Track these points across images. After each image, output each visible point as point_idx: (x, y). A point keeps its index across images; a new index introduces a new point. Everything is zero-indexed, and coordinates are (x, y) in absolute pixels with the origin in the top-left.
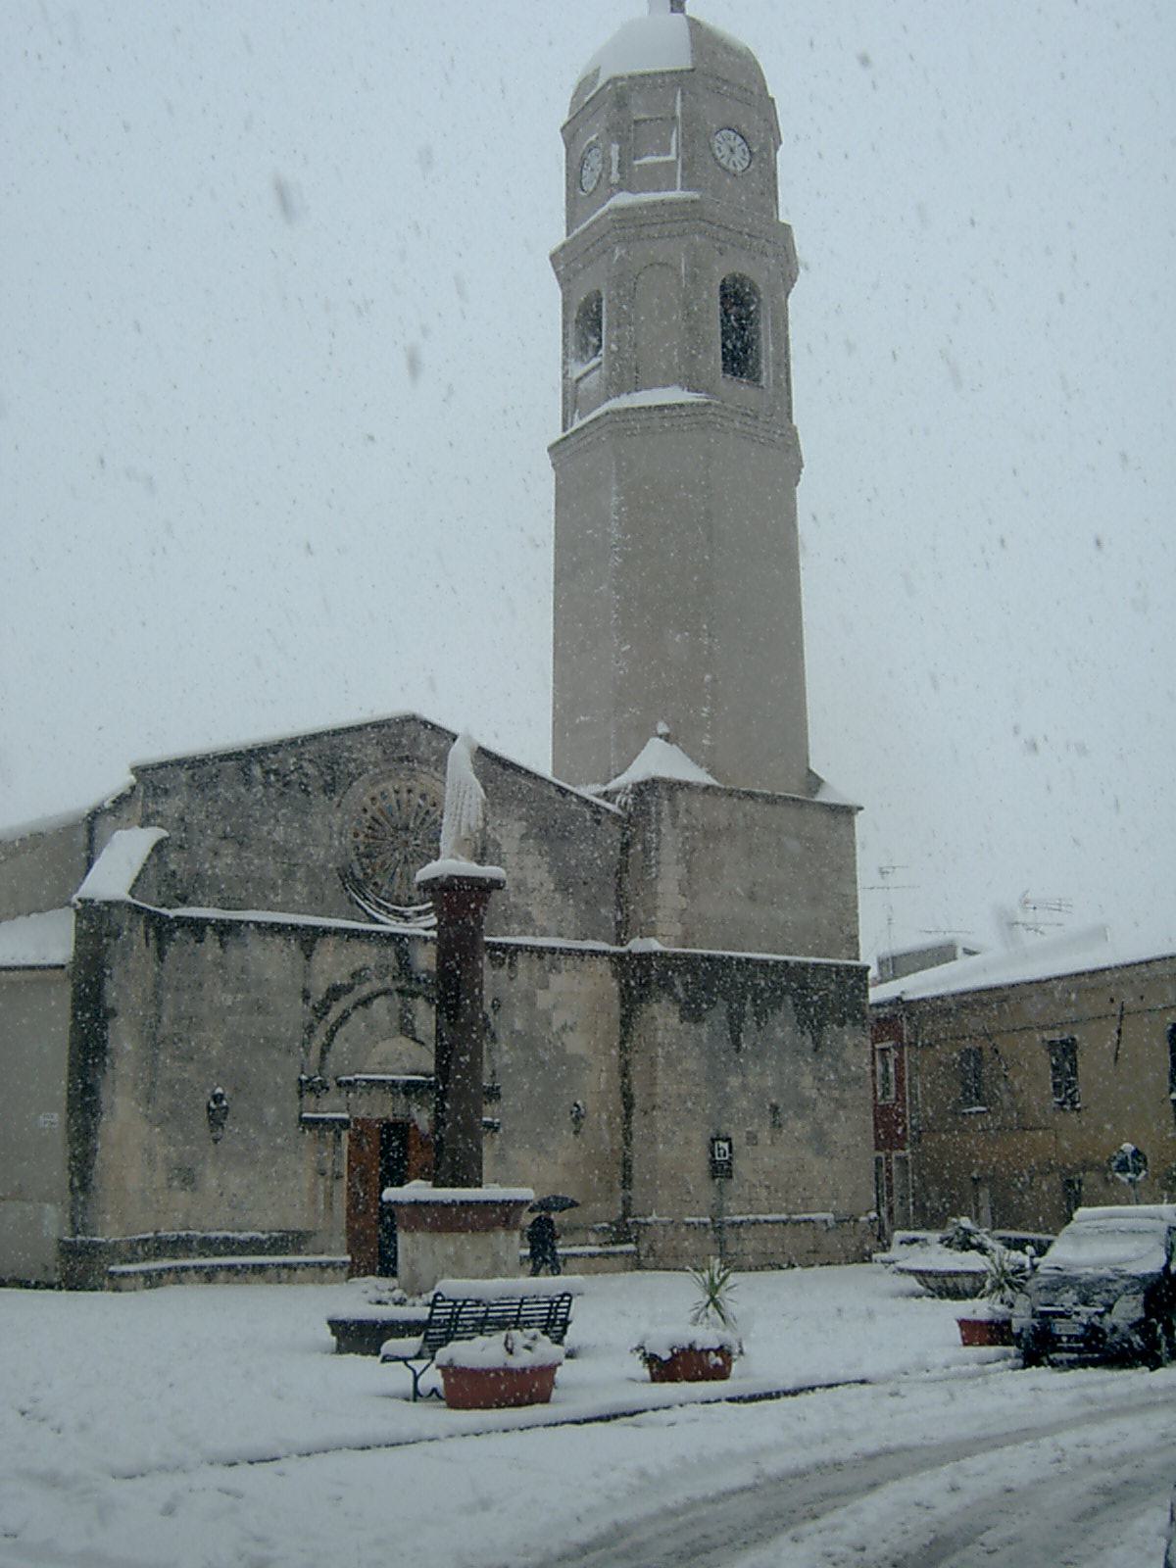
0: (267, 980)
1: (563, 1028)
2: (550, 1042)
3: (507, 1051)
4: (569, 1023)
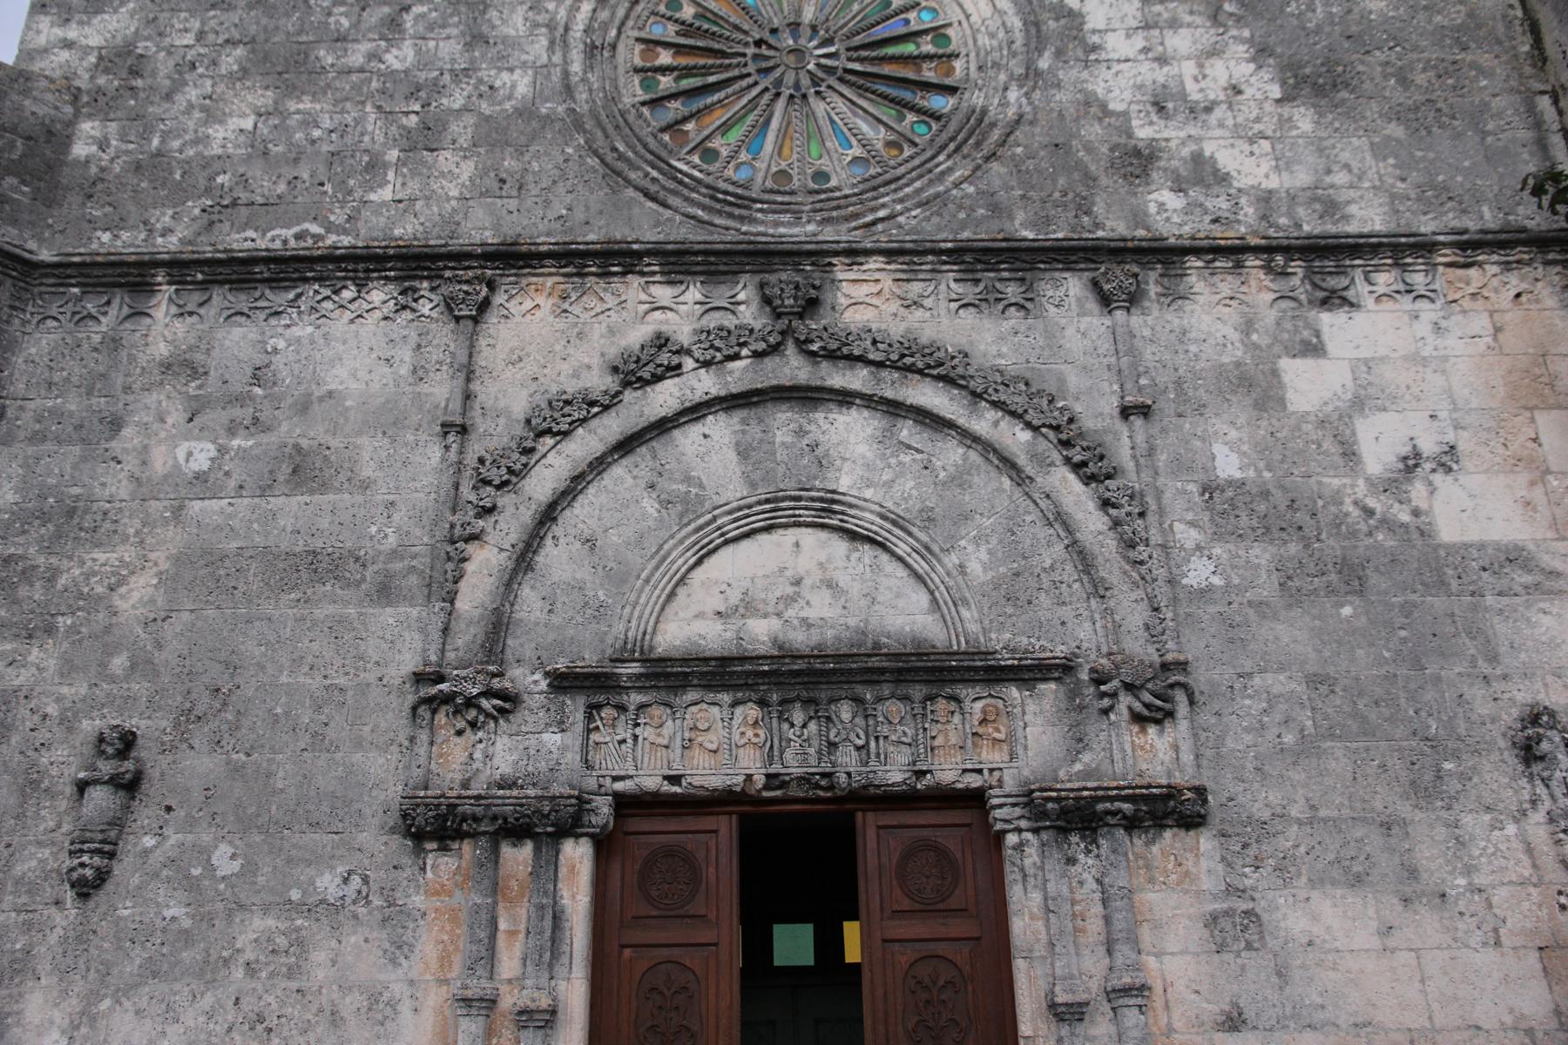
0: (330, 394)
1: (1411, 463)
2: (1369, 512)
3: (1198, 548)
4: (1428, 446)
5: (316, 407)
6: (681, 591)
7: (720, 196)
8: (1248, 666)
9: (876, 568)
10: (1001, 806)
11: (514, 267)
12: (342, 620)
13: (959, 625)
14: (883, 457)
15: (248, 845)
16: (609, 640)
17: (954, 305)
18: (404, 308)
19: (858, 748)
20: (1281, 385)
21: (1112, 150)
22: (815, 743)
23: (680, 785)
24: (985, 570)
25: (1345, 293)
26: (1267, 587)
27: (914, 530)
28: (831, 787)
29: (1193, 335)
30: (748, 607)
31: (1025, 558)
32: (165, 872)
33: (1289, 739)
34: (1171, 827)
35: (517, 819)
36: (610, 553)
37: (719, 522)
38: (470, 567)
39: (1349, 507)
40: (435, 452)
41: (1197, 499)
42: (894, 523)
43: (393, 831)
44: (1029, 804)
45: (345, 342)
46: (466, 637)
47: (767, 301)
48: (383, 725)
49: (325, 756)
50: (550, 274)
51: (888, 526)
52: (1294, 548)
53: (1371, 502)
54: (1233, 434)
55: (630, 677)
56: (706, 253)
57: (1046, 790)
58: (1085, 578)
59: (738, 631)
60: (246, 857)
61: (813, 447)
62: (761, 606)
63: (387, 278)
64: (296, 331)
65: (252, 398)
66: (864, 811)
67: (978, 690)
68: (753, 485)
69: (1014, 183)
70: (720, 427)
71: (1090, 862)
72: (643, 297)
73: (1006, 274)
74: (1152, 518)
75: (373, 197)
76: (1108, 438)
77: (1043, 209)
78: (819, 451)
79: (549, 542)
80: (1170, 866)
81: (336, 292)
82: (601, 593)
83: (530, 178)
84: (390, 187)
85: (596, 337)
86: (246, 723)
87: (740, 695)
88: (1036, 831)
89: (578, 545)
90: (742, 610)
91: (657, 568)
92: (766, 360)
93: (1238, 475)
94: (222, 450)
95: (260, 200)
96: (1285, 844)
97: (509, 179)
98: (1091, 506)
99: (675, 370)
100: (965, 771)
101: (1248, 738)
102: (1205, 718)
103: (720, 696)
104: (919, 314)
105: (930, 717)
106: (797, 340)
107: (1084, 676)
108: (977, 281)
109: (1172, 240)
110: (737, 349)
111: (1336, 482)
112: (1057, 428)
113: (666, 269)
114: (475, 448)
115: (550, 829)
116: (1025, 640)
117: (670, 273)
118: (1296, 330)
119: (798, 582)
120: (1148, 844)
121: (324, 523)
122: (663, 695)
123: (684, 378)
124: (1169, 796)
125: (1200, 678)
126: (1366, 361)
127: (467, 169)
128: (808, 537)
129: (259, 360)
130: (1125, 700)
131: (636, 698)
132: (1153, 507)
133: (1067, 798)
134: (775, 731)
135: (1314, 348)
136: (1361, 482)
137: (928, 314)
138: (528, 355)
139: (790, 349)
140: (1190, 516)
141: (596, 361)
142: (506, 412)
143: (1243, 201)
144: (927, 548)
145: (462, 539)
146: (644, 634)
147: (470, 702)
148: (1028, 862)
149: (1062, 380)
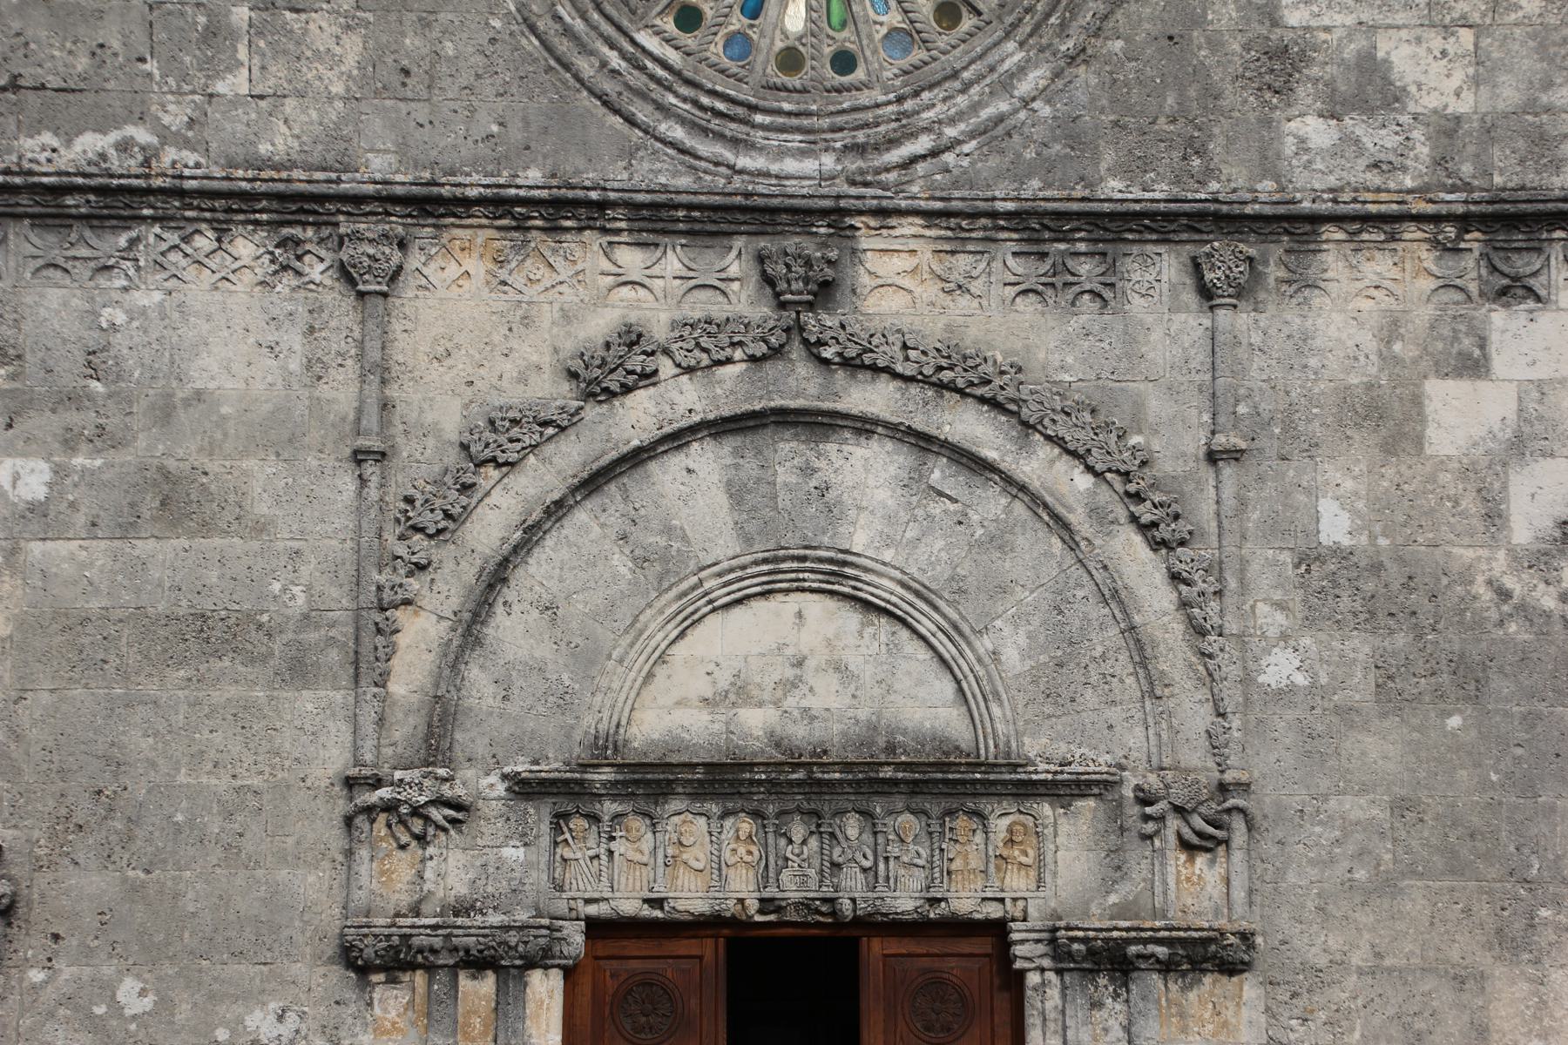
0: (199, 395)
2: (1504, 594)
3: (1284, 637)
5: (181, 413)
6: (661, 671)
7: (705, 100)
8: (1324, 784)
9: (893, 648)
10: (1022, 942)
11: (431, 215)
12: (248, 706)
13: (988, 725)
14: (910, 507)
15: (159, 979)
16: (578, 735)
17: (1011, 291)
18: (285, 268)
19: (864, 870)
20: (1422, 419)
21: (1247, 47)
22: (816, 862)
23: (662, 908)
24: (1023, 660)
25: (1532, 282)
26: (1360, 688)
27: (941, 604)
28: (833, 914)
29: (1318, 343)
30: (740, 692)
31: (1071, 643)
32: (62, 1012)
33: (1361, 874)
34: (1212, 971)
35: (481, 951)
36: (574, 625)
37: (707, 585)
38: (402, 640)
39: (1480, 588)
40: (348, 484)
41: (1290, 572)
42: (918, 594)
43: (331, 961)
44: (1053, 941)
45: (209, 318)
46: (405, 730)
47: (768, 280)
48: (311, 836)
49: (242, 873)
50: (481, 227)
51: (910, 597)
52: (1401, 640)
53: (1509, 582)
54: (1349, 484)
55: (604, 784)
56: (690, 207)
57: (1072, 929)
58: (1140, 671)
59: (727, 723)
60: (158, 993)
61: (823, 490)
62: (755, 692)
63: (257, 223)
64: (141, 298)
65: (91, 397)
66: (869, 937)
67: (1008, 805)
68: (748, 540)
69: (1104, 102)
70: (706, 458)
71: (1118, 1007)
72: (606, 265)
73: (1082, 247)
74: (1230, 600)
75: (220, 87)
76: (1189, 487)
77: (1140, 144)
78: (831, 496)
79: (499, 609)
80: (1207, 1015)
81: (186, 239)
82: (565, 676)
83: (443, 68)
84: (245, 72)
85: (546, 324)
86: (140, 833)
87: (730, 805)
88: (1059, 972)
89: (535, 614)
90: (732, 697)
91: (632, 645)
92: (768, 365)
93: (1346, 541)
94: (60, 472)
95: (54, 81)
96: (1339, 995)
97: (414, 69)
98: (1159, 577)
99: (648, 377)
100: (984, 899)
101: (1313, 873)
102: (1268, 847)
103: (707, 805)
104: (964, 301)
105: (948, 835)
106: (805, 342)
107: (1128, 792)
108: (1043, 256)
109: (1306, 205)
110: (729, 351)
111: (1469, 554)
112: (1126, 476)
113: (637, 225)
114: (400, 484)
115: (518, 962)
116: (1063, 747)
117: (640, 231)
118: (1456, 339)
119: (800, 663)
120: (1184, 989)
121: (213, 577)
122: (642, 805)
123: (661, 388)
124: (1210, 940)
125: (1262, 802)
126: (1539, 384)
127: (352, 49)
128: (816, 606)
129: (93, 339)
130: (1174, 823)
131: (609, 808)
132: (1232, 583)
133: (1095, 939)
134: (771, 849)
135: (1474, 366)
136: (1501, 555)
137: (975, 304)
138: (458, 346)
139: (796, 351)
140: (1277, 596)
141: (547, 360)
142: (434, 430)
143: (1417, 135)
144: (956, 628)
145: (388, 604)
146: (618, 726)
147: (416, 811)
148: (1049, 1005)
149: (1139, 406)
